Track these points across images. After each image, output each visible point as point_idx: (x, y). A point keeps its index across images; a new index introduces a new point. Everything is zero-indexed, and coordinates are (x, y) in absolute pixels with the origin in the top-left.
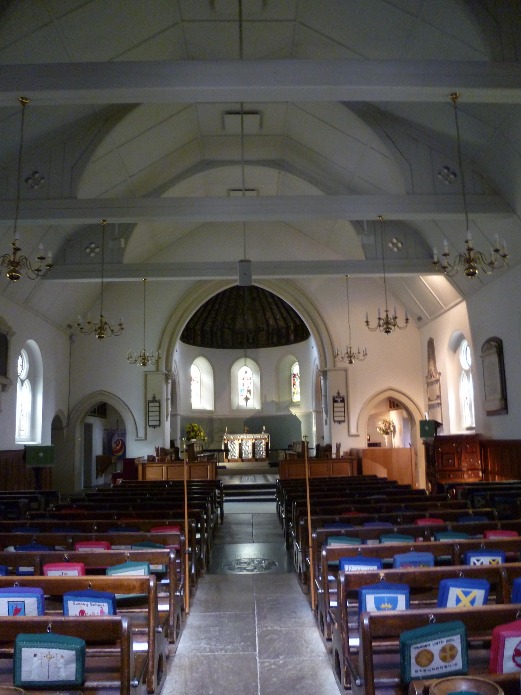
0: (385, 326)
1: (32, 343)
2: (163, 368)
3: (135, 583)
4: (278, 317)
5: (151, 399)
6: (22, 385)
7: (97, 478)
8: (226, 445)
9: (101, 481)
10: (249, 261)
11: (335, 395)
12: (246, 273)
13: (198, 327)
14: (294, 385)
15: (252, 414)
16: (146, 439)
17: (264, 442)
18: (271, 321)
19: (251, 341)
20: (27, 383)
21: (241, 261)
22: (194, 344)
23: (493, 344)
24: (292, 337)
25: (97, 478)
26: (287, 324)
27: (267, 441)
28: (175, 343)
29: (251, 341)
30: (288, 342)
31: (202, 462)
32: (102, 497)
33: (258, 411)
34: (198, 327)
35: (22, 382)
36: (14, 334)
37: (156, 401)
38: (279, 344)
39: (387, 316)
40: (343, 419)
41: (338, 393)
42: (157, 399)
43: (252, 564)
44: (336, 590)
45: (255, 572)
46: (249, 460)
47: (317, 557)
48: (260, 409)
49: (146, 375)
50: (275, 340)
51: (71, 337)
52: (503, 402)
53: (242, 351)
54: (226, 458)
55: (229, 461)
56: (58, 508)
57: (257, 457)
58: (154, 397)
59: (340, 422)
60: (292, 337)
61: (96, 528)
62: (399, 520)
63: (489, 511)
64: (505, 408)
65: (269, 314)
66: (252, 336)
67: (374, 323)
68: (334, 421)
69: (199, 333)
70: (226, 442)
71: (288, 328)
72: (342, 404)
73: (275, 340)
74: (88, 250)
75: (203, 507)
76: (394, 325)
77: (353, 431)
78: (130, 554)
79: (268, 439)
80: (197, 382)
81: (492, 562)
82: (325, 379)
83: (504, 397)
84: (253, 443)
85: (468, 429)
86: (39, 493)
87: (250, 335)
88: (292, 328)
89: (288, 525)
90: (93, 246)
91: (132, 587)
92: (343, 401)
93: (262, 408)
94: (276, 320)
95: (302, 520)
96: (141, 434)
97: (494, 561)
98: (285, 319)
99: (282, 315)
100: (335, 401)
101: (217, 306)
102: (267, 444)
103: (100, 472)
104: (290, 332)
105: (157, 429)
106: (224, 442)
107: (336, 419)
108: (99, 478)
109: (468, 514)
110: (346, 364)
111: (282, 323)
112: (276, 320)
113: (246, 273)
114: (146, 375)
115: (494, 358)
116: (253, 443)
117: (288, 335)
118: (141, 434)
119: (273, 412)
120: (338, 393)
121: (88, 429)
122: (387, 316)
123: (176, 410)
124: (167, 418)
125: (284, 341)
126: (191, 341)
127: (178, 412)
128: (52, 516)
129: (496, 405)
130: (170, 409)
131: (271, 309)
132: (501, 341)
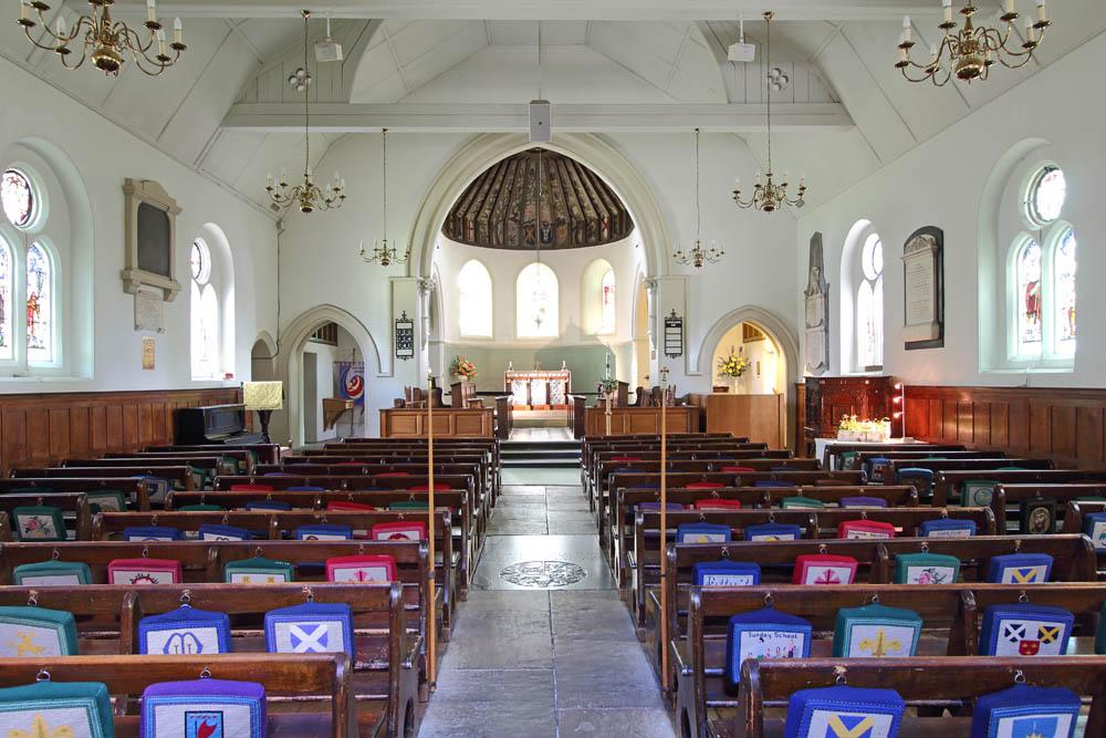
0: (766, 199)
1: (214, 227)
2: (416, 272)
3: (304, 669)
4: (587, 202)
5: (400, 317)
6: (201, 292)
7: (325, 430)
8: (508, 385)
9: (331, 434)
10: (546, 102)
11: (669, 316)
12: (541, 125)
13: (470, 216)
15: (547, 343)
16: (393, 375)
17: (563, 383)
18: (576, 210)
19: (546, 239)
20: (209, 289)
21: (533, 102)
22: (465, 241)
23: (927, 237)
24: (606, 233)
25: (325, 430)
26: (598, 214)
28: (435, 235)
29: (546, 239)
30: (600, 241)
31: (475, 409)
32: (310, 465)
33: (556, 340)
34: (470, 216)
35: (201, 287)
36: (179, 211)
37: (407, 321)
38: (586, 244)
39: (770, 183)
40: (678, 351)
41: (673, 314)
42: (408, 317)
43: (547, 573)
44: (720, 671)
45: (551, 587)
46: (542, 408)
47: (675, 596)
49: (392, 282)
50: (580, 236)
51: (278, 224)
52: (937, 327)
53: (534, 253)
56: (225, 485)
57: (553, 403)
58: (404, 315)
59: (674, 355)
60: (606, 233)
61: (276, 524)
62: (811, 521)
63: (979, 512)
64: (939, 340)
65: (573, 199)
67: (746, 197)
68: (667, 354)
69: (472, 226)
71: (600, 219)
72: (678, 330)
73: (580, 236)
74: (294, 81)
75: (466, 486)
76: (780, 200)
77: (693, 368)
78: (314, 589)
81: (1044, 631)
82: (654, 293)
83: (940, 323)
85: (869, 369)
86: (192, 463)
88: (606, 220)
89: (602, 510)
90: (301, 73)
91: (299, 678)
92: (679, 326)
93: (561, 336)
94: (582, 207)
95: (640, 517)
96: (386, 369)
97: (1049, 629)
98: (595, 207)
99: (592, 200)
100: (668, 326)
101: (497, 186)
102: (567, 384)
103: (328, 423)
104: (603, 226)
105: (410, 360)
107: (669, 351)
108: (328, 431)
109: (938, 516)
110: (690, 269)
111: (591, 213)
112: (582, 207)
113: (541, 125)
114: (392, 282)
115: (927, 260)
117: (600, 231)
118: (386, 369)
119: (576, 341)
120: (673, 314)
121: (310, 359)
122: (770, 183)
123: (438, 336)
124: (423, 346)
126: (460, 237)
127: (441, 340)
128: (211, 501)
129: (927, 333)
130: (428, 333)
131: (576, 191)
132: (942, 232)
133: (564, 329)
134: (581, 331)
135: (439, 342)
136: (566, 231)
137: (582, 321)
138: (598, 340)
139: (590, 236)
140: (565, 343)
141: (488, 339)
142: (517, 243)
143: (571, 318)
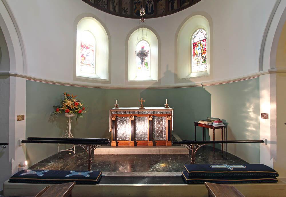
14: (194, 55)
19: (149, 11)
27: (169, 119)
29: (149, 11)
33: (155, 82)
48: (158, 80)
54: (113, 140)
55: (117, 146)
66: (151, 6)
70: (114, 119)
79: (171, 116)
80: (93, 50)
84: (150, 120)
87: (148, 6)
93: (160, 80)
102: (169, 122)
106: (111, 119)
116: (150, 120)
125: (186, 4)
133: (162, 76)
134: (176, 75)
135: (9, 75)
136: (164, 4)
137: (176, 69)
138: (191, 82)
139: (184, 2)
140: (163, 85)
141: (103, 81)
142: (129, 13)
143: (167, 66)
